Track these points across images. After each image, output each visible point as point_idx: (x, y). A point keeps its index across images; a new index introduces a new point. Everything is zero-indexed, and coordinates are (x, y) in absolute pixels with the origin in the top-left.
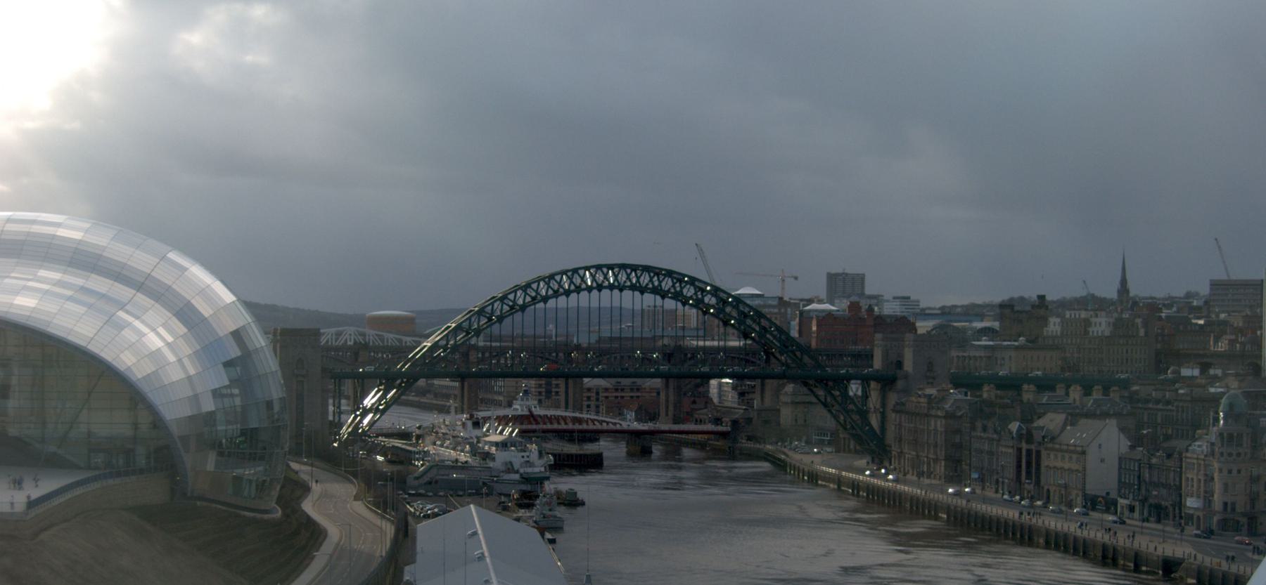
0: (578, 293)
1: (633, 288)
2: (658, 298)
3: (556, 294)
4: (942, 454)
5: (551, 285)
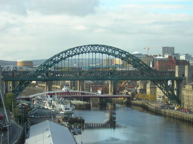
0: (82, 54)
1: (99, 52)
2: (107, 55)
3: (75, 54)
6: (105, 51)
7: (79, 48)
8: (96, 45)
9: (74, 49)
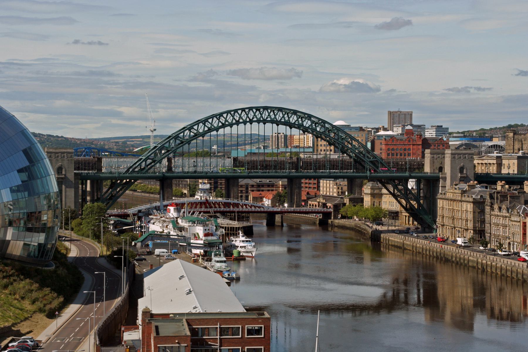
0: (238, 125)
1: (272, 122)
2: (288, 128)
3: (224, 126)
4: (470, 225)
5: (221, 120)
6: (283, 120)
7: (232, 113)
8: (266, 108)
9: (221, 115)
